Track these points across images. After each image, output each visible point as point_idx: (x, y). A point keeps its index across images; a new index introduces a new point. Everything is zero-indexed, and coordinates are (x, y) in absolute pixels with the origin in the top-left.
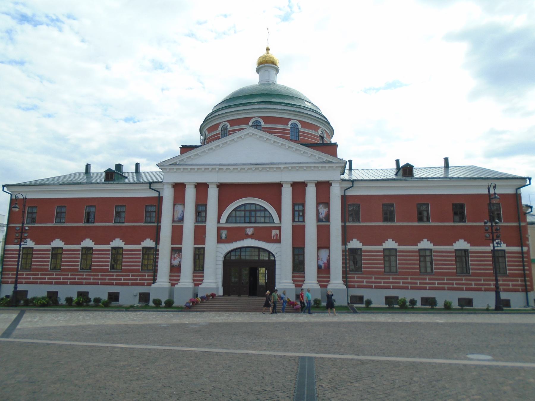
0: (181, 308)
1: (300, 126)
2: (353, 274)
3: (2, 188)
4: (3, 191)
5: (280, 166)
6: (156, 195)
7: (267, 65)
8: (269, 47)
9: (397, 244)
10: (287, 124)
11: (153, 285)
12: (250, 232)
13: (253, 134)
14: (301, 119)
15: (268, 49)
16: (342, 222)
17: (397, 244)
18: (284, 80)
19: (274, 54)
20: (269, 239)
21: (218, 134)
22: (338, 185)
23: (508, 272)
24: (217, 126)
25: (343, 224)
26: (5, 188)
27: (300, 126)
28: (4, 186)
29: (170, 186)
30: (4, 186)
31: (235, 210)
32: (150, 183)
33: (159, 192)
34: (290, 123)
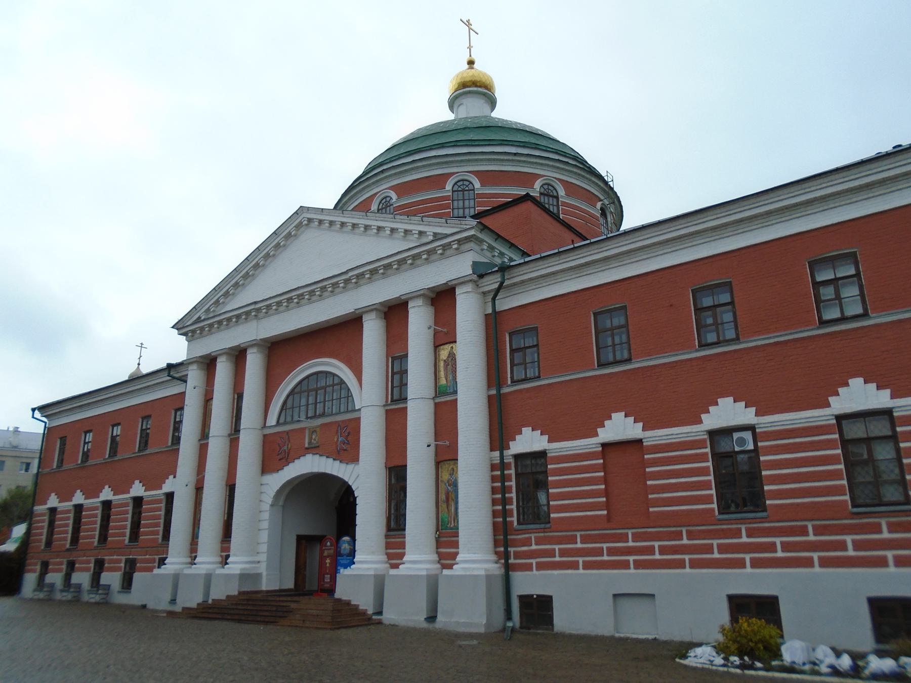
3: (31, 413)
4: (33, 417)
5: (350, 274)
9: (640, 425)
11: (156, 571)
13: (310, 220)
16: (489, 386)
17: (640, 425)
18: (510, 109)
22: (469, 287)
25: (493, 392)
26: (36, 412)
28: (33, 410)
30: (33, 410)
31: (292, 392)
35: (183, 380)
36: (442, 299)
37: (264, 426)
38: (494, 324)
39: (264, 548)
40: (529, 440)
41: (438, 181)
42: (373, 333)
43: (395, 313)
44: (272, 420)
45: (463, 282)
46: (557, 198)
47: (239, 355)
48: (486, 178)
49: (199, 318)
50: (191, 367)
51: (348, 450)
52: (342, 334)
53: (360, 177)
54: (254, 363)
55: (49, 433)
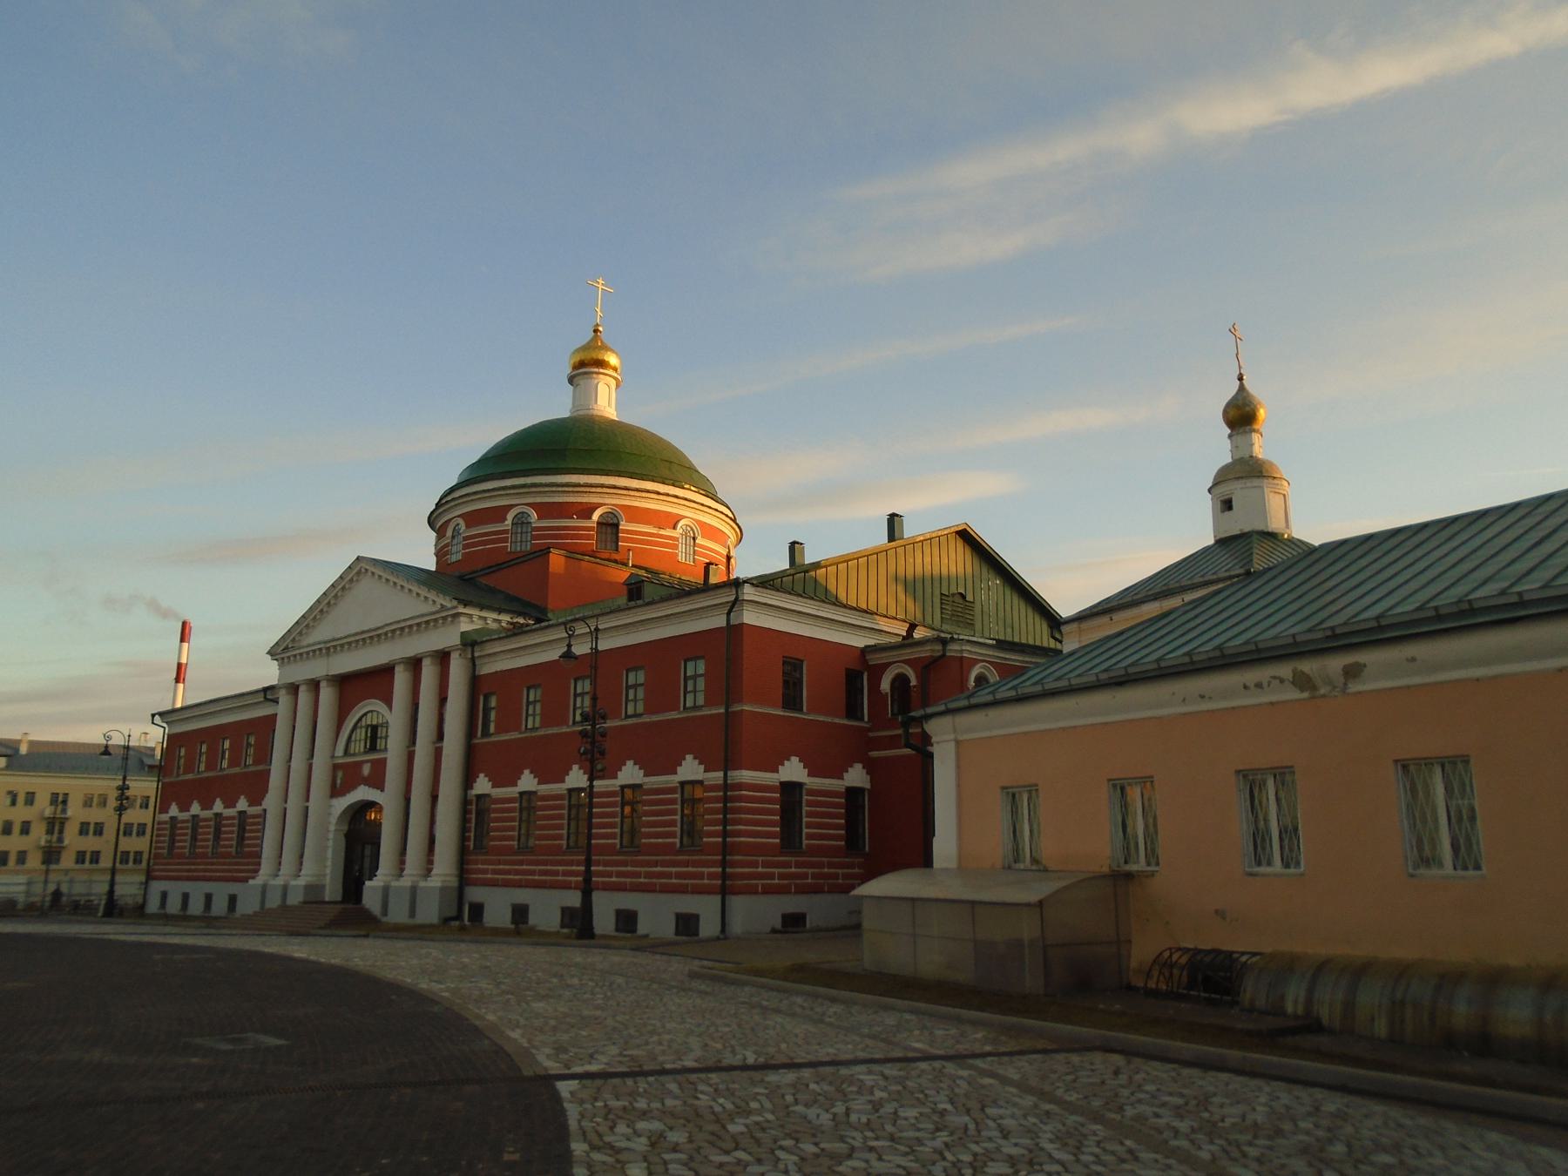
0: (431, 926)
12: (366, 770)
14: (538, 500)
23: (805, 842)
34: (510, 516)
35: (276, 701)
36: (443, 657)
37: (333, 757)
38: (476, 684)
39: (329, 863)
40: (482, 785)
41: (499, 514)
42: (401, 679)
43: (415, 664)
44: (340, 751)
45: (455, 648)
46: (617, 526)
47: (315, 685)
48: (545, 510)
51: (377, 781)
52: (375, 681)
53: (452, 490)
54: (327, 694)
55: (173, 741)
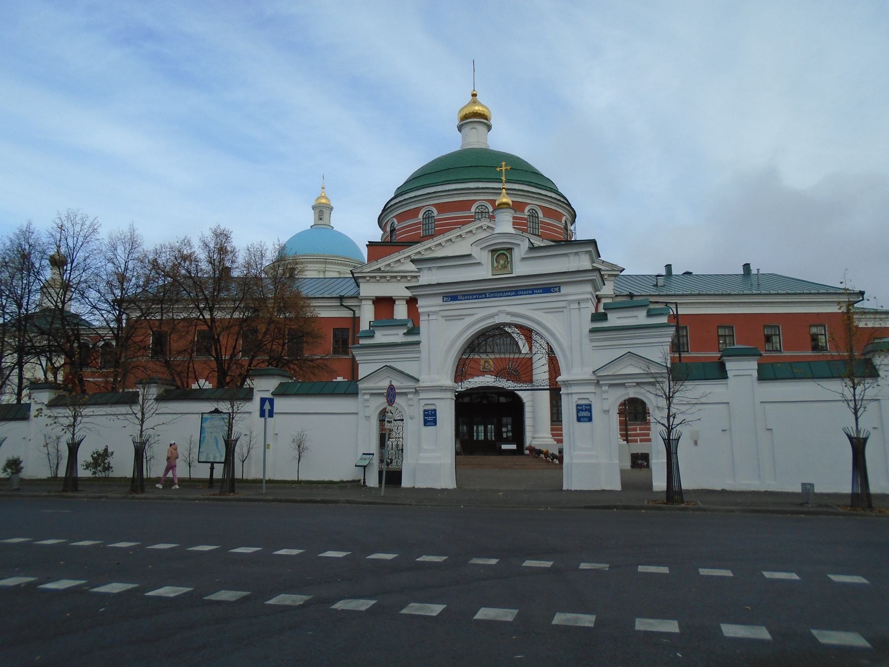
1: (541, 215)
2: (633, 425)
6: (347, 314)
7: (474, 119)
8: (477, 92)
10: (523, 211)
13: (488, 227)
15: (474, 95)
19: (486, 103)
20: (516, 378)
21: (419, 223)
24: (414, 213)
27: (541, 215)
29: (371, 302)
32: (341, 298)
33: (354, 311)
49: (380, 269)
50: (364, 302)
